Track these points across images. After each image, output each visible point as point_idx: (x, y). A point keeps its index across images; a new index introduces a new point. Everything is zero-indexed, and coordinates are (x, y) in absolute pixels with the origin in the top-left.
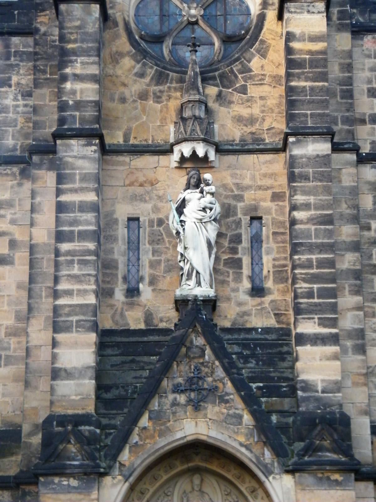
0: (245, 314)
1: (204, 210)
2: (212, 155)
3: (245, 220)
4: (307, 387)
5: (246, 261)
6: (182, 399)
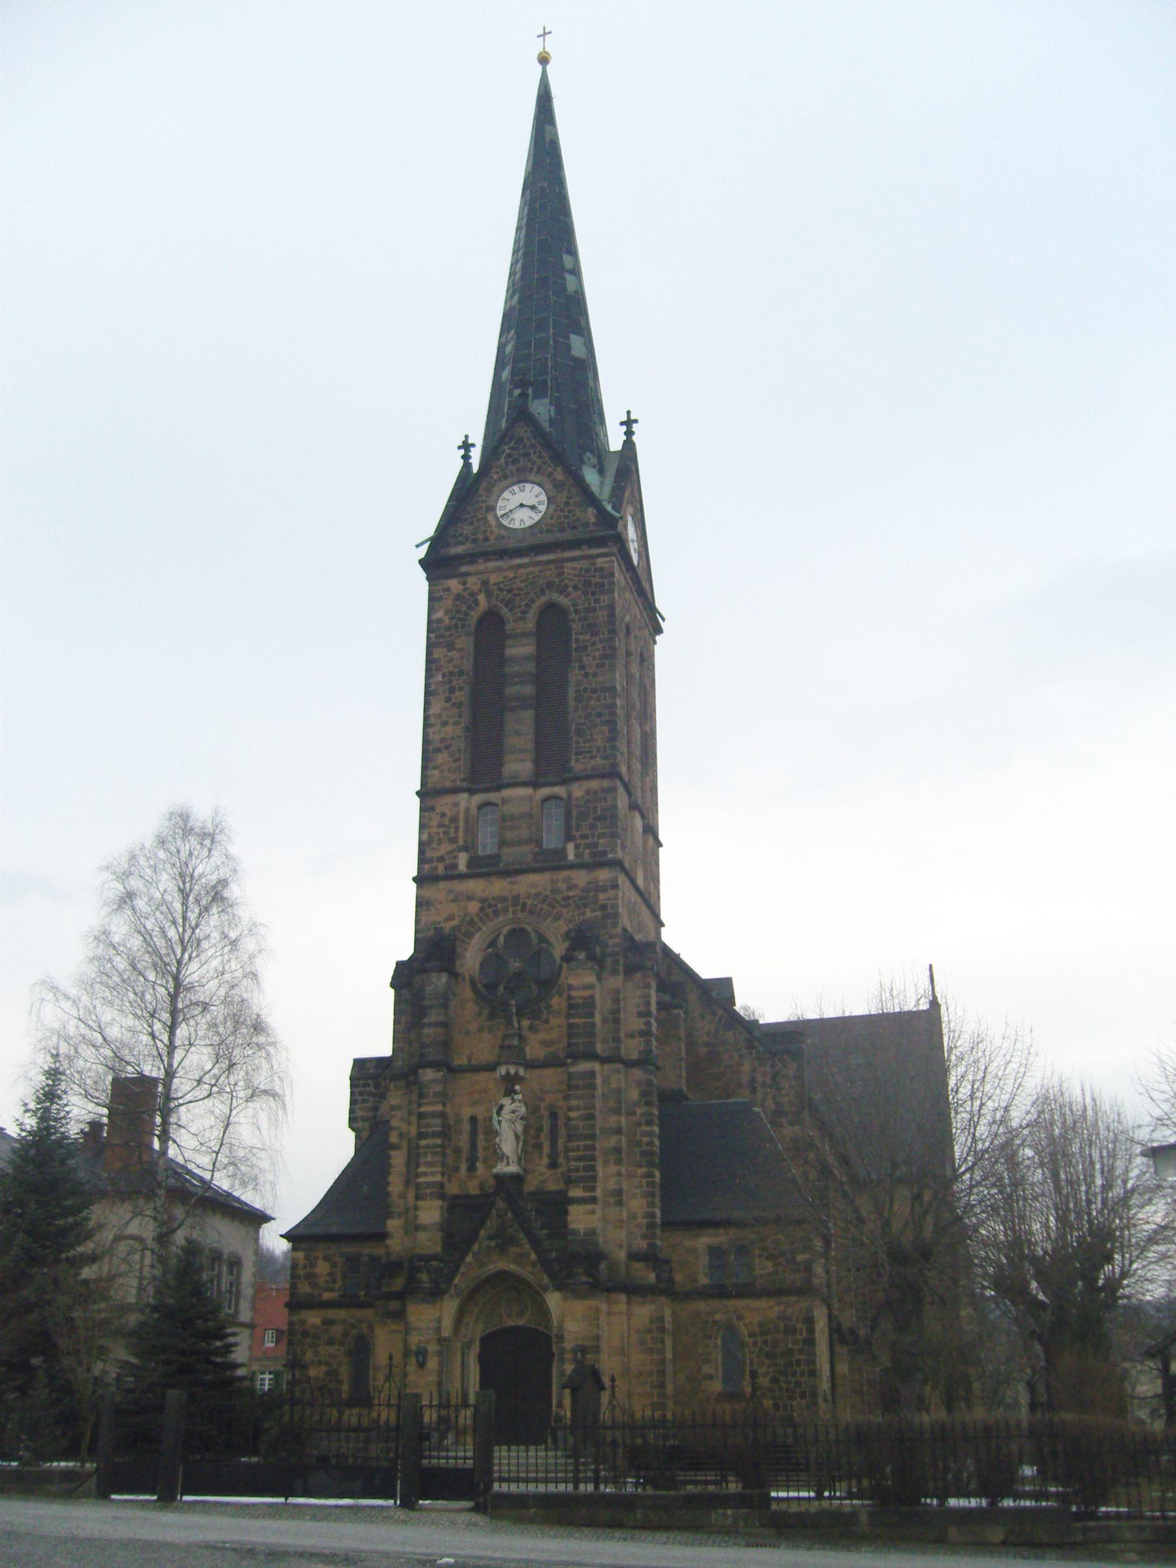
0: (544, 1181)
1: (513, 1112)
2: (521, 1072)
3: (546, 1114)
4: (575, 1233)
5: (546, 1144)
6: (493, 1244)
